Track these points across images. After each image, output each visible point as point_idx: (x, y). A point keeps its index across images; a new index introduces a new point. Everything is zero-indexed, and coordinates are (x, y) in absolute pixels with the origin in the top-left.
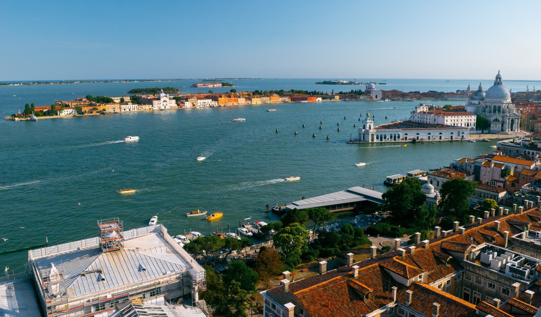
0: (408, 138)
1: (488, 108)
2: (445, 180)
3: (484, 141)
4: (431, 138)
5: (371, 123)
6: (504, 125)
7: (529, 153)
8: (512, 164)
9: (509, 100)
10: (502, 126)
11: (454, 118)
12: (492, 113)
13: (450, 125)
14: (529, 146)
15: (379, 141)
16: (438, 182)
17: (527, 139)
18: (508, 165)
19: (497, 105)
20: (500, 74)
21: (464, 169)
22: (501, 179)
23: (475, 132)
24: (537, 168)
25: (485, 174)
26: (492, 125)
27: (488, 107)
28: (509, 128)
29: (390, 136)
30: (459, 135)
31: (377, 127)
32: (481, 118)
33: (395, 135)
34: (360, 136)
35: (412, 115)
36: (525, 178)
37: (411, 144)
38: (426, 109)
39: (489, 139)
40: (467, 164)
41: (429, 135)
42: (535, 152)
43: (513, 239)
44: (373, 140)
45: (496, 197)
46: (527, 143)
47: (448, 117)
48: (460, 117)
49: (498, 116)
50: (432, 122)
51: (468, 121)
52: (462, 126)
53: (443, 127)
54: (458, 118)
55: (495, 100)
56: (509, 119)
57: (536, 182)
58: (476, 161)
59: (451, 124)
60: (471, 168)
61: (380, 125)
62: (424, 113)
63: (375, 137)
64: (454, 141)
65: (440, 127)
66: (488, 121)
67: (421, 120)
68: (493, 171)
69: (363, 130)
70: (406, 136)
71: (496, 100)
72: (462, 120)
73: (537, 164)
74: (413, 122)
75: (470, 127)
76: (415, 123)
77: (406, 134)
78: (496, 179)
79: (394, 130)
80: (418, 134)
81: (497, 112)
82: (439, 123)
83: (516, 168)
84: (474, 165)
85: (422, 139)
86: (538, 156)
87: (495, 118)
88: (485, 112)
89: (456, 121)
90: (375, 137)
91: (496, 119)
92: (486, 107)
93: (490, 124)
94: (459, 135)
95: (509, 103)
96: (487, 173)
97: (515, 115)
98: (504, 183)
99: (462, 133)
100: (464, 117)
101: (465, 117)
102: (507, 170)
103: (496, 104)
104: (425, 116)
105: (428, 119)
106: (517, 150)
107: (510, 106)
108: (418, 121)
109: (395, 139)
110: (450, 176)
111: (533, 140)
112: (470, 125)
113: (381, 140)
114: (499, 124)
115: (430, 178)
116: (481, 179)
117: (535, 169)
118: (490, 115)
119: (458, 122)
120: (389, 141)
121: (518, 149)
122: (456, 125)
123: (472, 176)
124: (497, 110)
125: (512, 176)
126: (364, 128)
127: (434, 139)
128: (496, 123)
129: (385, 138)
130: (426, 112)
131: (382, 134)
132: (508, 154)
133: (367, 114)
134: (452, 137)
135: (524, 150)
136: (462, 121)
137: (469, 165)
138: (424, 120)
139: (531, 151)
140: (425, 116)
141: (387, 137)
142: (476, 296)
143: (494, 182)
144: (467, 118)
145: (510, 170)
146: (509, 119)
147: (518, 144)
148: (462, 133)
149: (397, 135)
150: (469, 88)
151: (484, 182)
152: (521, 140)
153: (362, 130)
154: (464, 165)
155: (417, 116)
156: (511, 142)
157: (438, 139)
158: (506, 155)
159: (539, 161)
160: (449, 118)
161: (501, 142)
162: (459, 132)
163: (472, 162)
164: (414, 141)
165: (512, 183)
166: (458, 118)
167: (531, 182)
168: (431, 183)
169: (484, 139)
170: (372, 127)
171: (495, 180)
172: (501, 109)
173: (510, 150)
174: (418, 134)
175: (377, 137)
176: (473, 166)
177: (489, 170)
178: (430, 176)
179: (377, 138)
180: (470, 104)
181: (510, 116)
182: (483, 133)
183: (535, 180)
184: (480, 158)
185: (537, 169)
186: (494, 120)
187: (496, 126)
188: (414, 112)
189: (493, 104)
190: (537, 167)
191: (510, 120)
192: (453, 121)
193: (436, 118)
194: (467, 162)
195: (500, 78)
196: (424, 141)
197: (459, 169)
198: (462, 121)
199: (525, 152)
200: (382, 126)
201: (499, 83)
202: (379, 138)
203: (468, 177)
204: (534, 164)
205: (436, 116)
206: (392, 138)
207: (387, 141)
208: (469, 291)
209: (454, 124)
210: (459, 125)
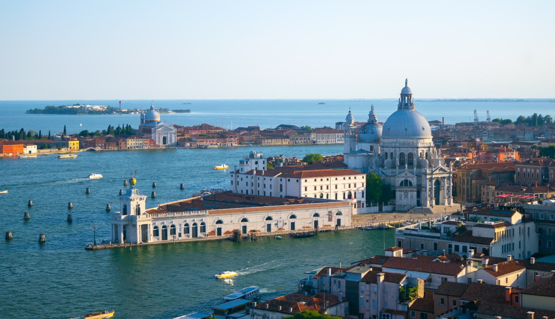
0: (223, 231)
1: (389, 159)
3: (381, 228)
4: (272, 226)
5: (141, 199)
6: (423, 193)
7: (457, 248)
8: (419, 273)
9: (428, 140)
10: (419, 196)
11: (322, 183)
12: (397, 168)
13: (313, 197)
14: (457, 234)
15: (159, 240)
17: (453, 220)
18: (413, 276)
19: (406, 152)
20: (408, 86)
21: (326, 291)
22: (400, 308)
23: (365, 209)
24: (471, 279)
25: (367, 298)
26: (398, 194)
27: (389, 156)
28: (431, 199)
29: (183, 227)
30: (330, 220)
31: (156, 208)
32: (376, 180)
33: (195, 224)
34: (117, 232)
35: (233, 179)
36: (446, 301)
37: (231, 243)
38: (264, 166)
39: (391, 225)
40: (332, 280)
41: (269, 222)
42: (468, 245)
44: (145, 238)
46: (453, 228)
47: (308, 180)
48: (333, 178)
49: (409, 175)
50: (276, 193)
51: (350, 187)
52: (338, 199)
53: (298, 203)
54: (328, 183)
55: (401, 141)
56: (431, 179)
57: (464, 307)
58: (350, 271)
59: (315, 196)
60: (339, 287)
61: (161, 205)
62: (259, 173)
63: (151, 230)
64: (321, 232)
65: (291, 203)
66: (389, 186)
67: (253, 188)
68: (384, 292)
69: (123, 217)
70: (219, 226)
71: (404, 140)
72: (336, 186)
73: (469, 271)
74: (237, 195)
75: (355, 201)
76: (241, 196)
77: (220, 222)
78: (392, 308)
79: (192, 214)
80: (245, 220)
81: (406, 166)
82: (290, 194)
83: (428, 281)
84: (346, 281)
85: (254, 231)
86: (473, 253)
87: (403, 179)
88: (383, 166)
89: (324, 187)
90: (151, 230)
91: (406, 181)
92: (384, 157)
93: (394, 192)
94: (330, 220)
95: (429, 147)
96: (373, 295)
97: (441, 172)
98: (406, 314)
99: (337, 214)
100: (340, 178)
101: (342, 178)
102: (411, 284)
103: (403, 150)
104: (261, 181)
105: (268, 186)
106: (436, 245)
107: (431, 151)
108: (247, 191)
109: (195, 235)
110: (296, 309)
111: (464, 221)
113: (165, 237)
114: (411, 191)
115: (255, 316)
116: (361, 310)
117: (467, 282)
118: (395, 173)
119: (328, 191)
120: (184, 237)
121: (436, 240)
122: (325, 197)
123: (343, 304)
124: (406, 162)
125: (419, 300)
126: (125, 213)
127: (280, 229)
128: (406, 189)
129: (173, 232)
130: (261, 171)
131: (166, 223)
132: (418, 253)
133: (131, 181)
134: (316, 223)
135: (448, 242)
136: (336, 188)
137: (335, 281)
138: (258, 189)
139: (461, 245)
140: (261, 181)
141: (178, 231)
143: (386, 314)
144: (347, 181)
145: (416, 285)
147: (436, 230)
148: (337, 214)
149: (199, 226)
150: (349, 118)
151: (367, 316)
152: (441, 223)
153: (120, 217)
154: (326, 280)
155: (245, 180)
156: (424, 228)
157: (287, 229)
158: (413, 256)
159: (472, 264)
160: (311, 180)
161: (403, 228)
162: (330, 212)
163: (343, 274)
164: (235, 237)
165: (422, 315)
166: (328, 183)
167: (456, 308)
169: (383, 225)
170: (143, 210)
171: (388, 311)
172: (415, 160)
173: (422, 245)
174: (245, 220)
175: (154, 231)
176: (343, 282)
177: (375, 289)
178: (255, 311)
179: (156, 233)
180: (353, 152)
181: (432, 174)
182: (381, 211)
183: (463, 303)
184: (359, 265)
185: (470, 279)
186: (401, 184)
187: (406, 196)
188: (238, 172)
189: (398, 149)
190: (469, 276)
191: (434, 181)
192: (318, 188)
194: (333, 275)
196: (258, 234)
197: (316, 291)
198: (336, 188)
199: (450, 246)
200: (167, 205)
201: (407, 105)
202: (160, 233)
203: (334, 308)
204: (464, 270)
205: (284, 179)
206: (188, 233)
207: (178, 239)
210: (333, 197)
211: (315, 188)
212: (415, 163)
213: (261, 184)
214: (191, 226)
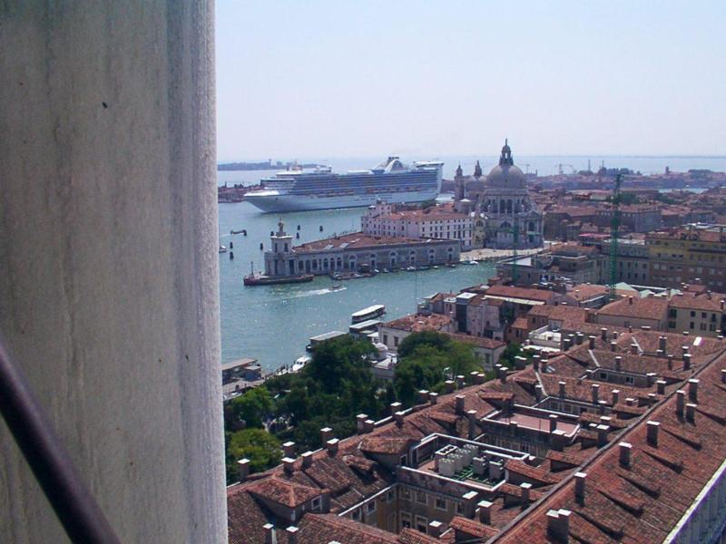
2: (406, 334)
10: (516, 236)
16: (396, 339)
19: (506, 199)
26: (499, 234)
43: (485, 421)
45: (491, 358)
63: (296, 265)
81: (506, 210)
89: (439, 228)
103: (503, 198)
105: (392, 228)
112: (462, 235)
116: (469, 329)
142: (422, 524)
146: (525, 223)
150: (459, 171)
151: (473, 331)
168: (385, 343)
178: (383, 329)
187: (506, 236)
192: (434, 229)
193: (404, 225)
195: (509, 153)
208: (408, 516)
209: (436, 235)
210: (446, 237)
211: (431, 228)
212: (513, 207)
213: (387, 227)
214: (329, 261)
